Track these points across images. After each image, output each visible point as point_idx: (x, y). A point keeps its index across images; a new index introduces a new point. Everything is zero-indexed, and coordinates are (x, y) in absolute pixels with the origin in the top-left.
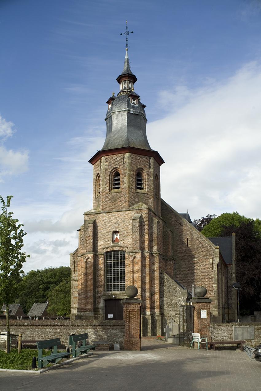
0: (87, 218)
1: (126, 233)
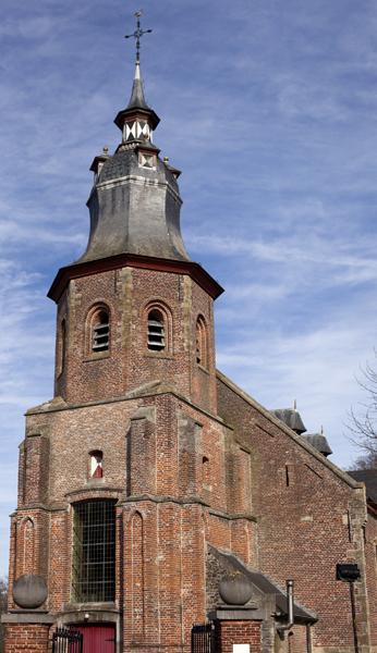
0: (32, 420)
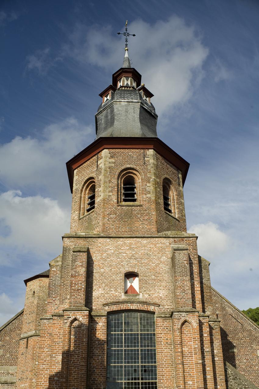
1: (153, 277)
